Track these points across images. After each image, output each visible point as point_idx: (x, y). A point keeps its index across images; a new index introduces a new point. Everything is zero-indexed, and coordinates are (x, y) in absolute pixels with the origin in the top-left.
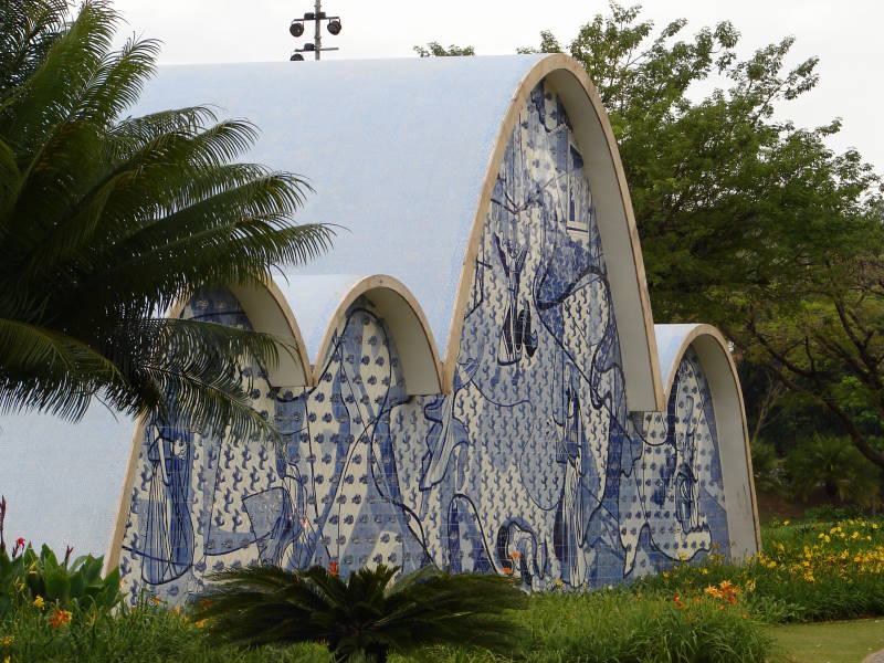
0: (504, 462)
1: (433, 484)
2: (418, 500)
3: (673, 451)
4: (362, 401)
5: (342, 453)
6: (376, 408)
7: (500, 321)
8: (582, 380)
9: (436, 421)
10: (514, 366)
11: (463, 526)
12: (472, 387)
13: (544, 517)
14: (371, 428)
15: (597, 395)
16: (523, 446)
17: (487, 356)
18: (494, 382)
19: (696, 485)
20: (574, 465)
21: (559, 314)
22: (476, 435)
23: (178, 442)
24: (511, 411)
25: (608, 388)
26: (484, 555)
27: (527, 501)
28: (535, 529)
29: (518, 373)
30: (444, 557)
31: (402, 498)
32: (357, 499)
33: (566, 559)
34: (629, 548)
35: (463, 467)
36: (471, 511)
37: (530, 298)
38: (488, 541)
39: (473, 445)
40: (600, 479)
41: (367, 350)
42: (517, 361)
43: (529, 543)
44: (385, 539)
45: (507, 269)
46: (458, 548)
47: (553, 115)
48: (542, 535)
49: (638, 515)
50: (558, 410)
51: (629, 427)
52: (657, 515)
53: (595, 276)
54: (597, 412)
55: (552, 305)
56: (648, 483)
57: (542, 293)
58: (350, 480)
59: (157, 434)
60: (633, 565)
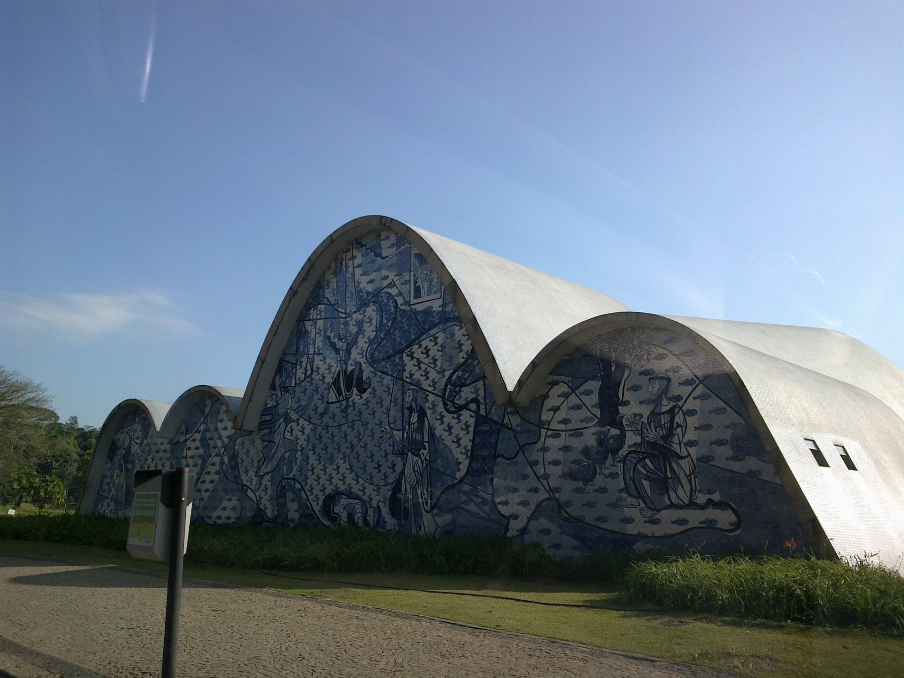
0: (332, 459)
1: (265, 473)
2: (254, 482)
3: (614, 432)
4: (217, 438)
5: (204, 461)
6: (226, 441)
7: (329, 380)
8: (431, 398)
9: (270, 441)
10: (344, 403)
11: (290, 495)
12: (302, 421)
13: (378, 491)
14: (223, 450)
15: (454, 403)
16: (352, 447)
17: (316, 401)
18: (322, 415)
19: (685, 463)
20: (419, 456)
21: (397, 361)
22: (303, 446)
23: (129, 464)
24: (340, 429)
25: (474, 396)
26: (310, 512)
27: (357, 480)
28: (364, 498)
29: (347, 407)
30: (273, 510)
31: (242, 481)
32: (212, 482)
33: (406, 519)
34: (515, 517)
35: (292, 463)
36: (298, 486)
37: (363, 361)
38: (314, 504)
39: (301, 451)
40: (460, 463)
41: (222, 416)
42: (347, 399)
43: (358, 508)
44: (230, 500)
45: (337, 351)
46: (286, 506)
47: (391, 246)
48: (374, 504)
49: (535, 490)
50: (395, 422)
51: (515, 420)
52: (578, 490)
53: (449, 324)
54: (455, 416)
55: (389, 357)
56: (556, 463)
57: (376, 353)
58: (209, 473)
59: (122, 461)
60: (523, 531)
